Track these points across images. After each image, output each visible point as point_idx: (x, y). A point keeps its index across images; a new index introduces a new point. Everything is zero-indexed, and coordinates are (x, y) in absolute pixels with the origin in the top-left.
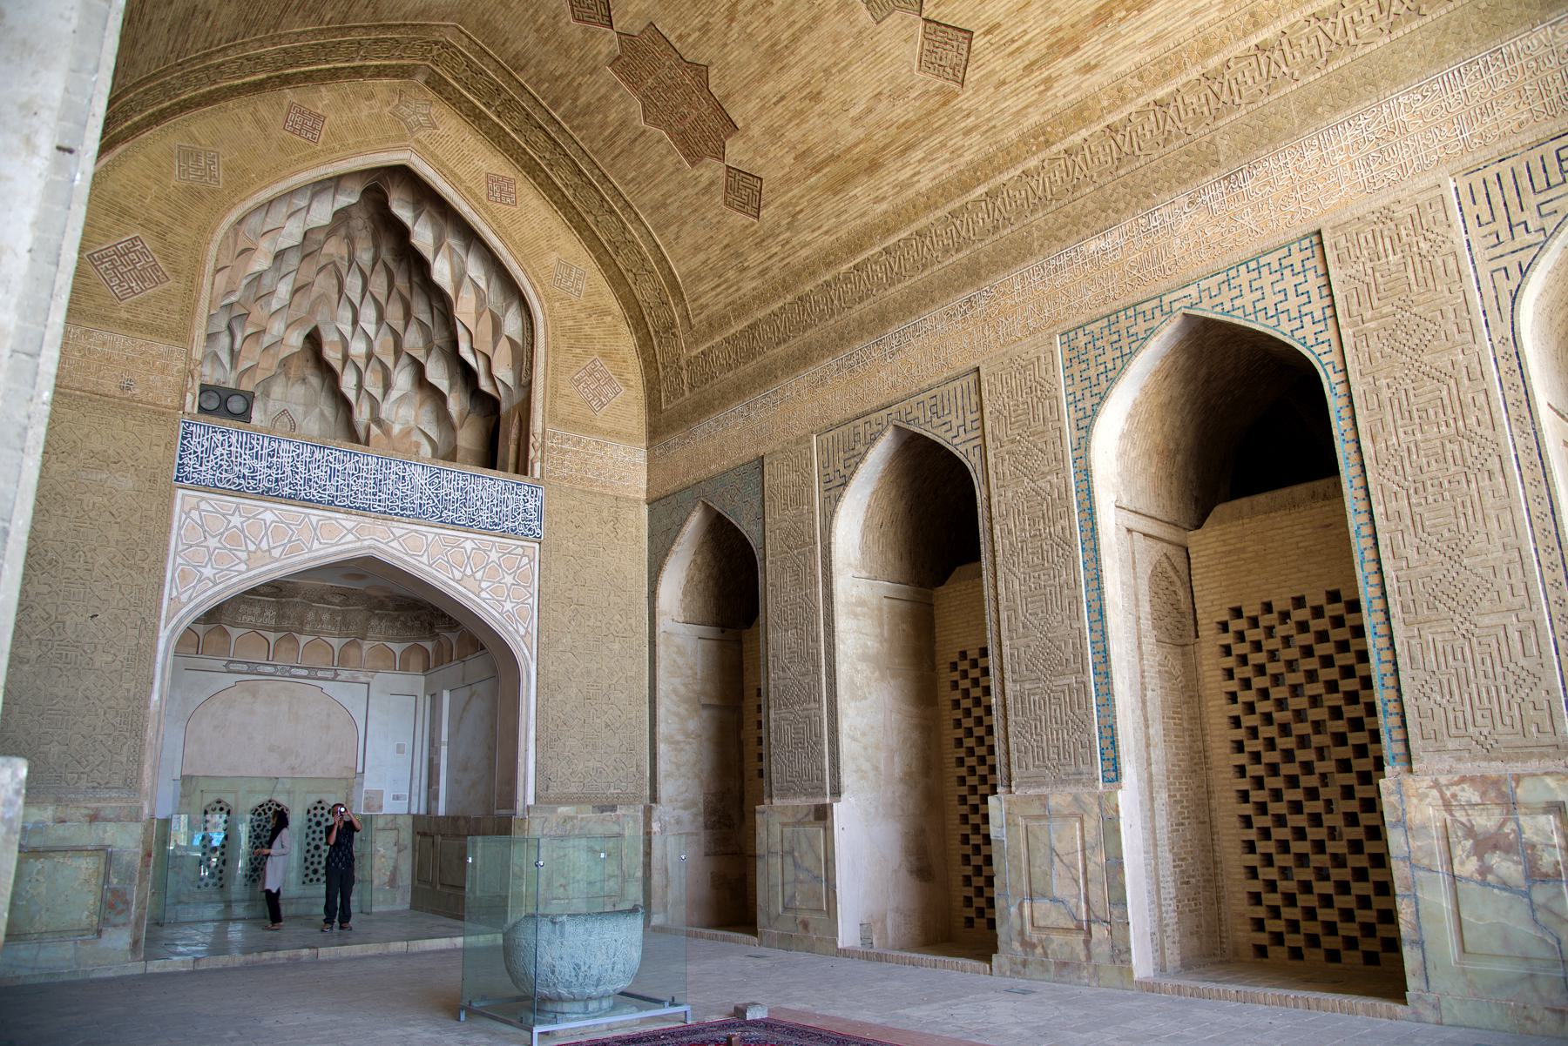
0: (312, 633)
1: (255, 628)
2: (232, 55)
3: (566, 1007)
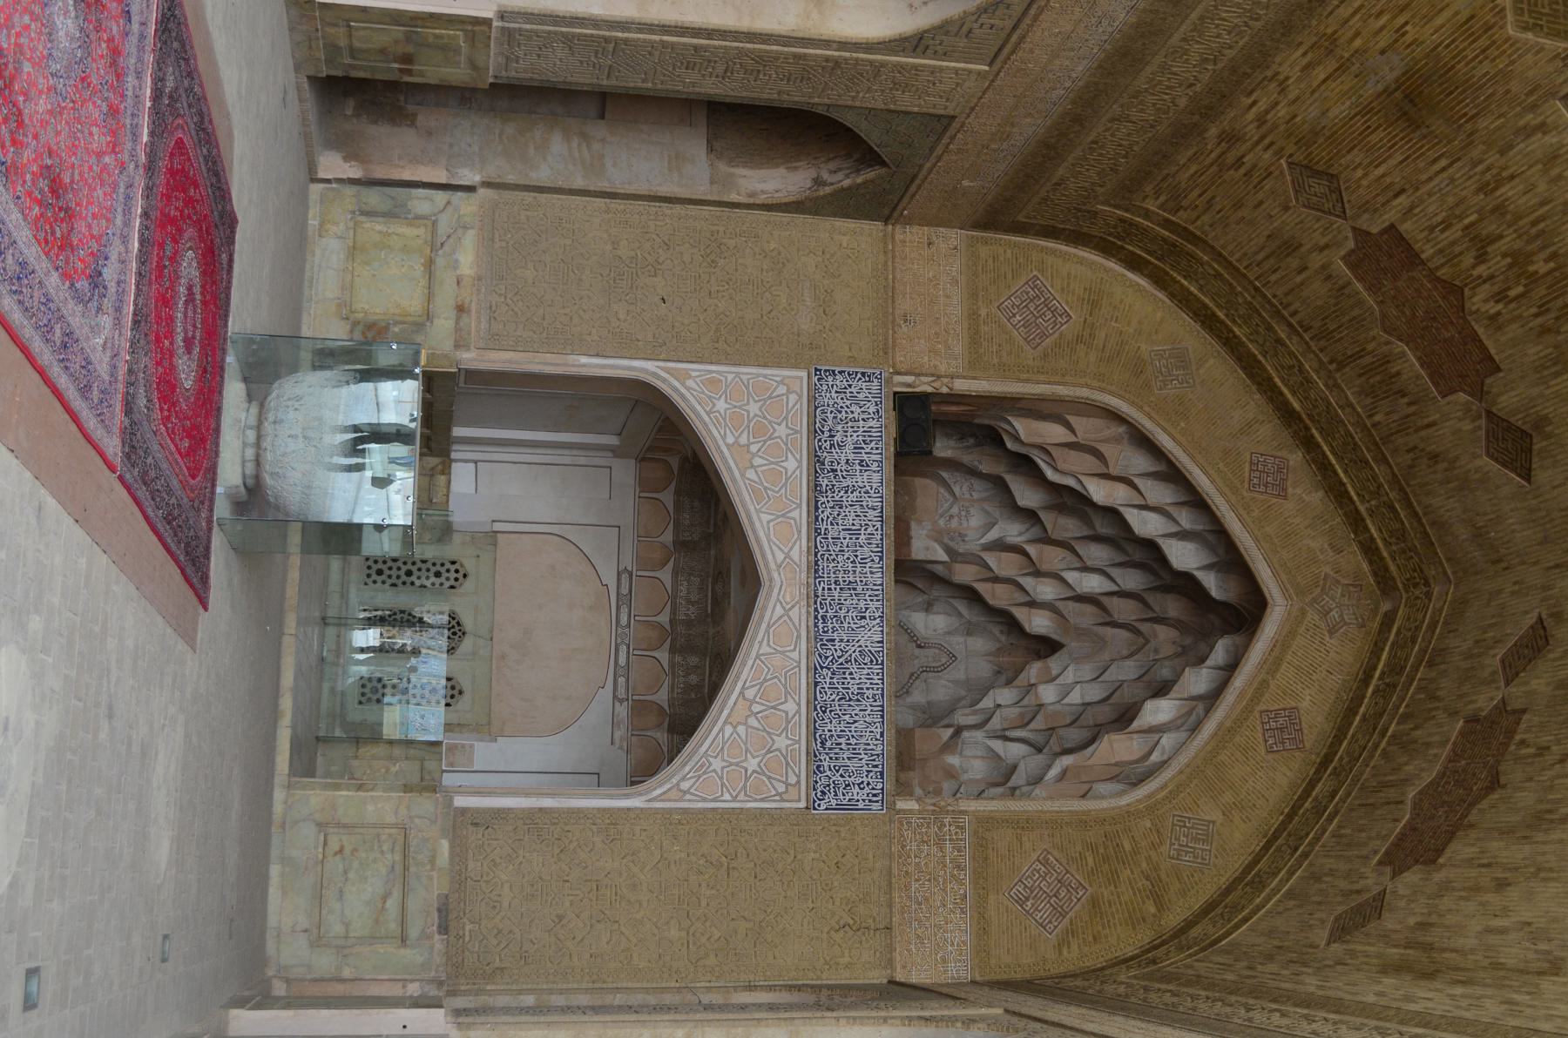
0: (672, 665)
1: (673, 597)
2: (1293, 345)
3: (254, 410)
